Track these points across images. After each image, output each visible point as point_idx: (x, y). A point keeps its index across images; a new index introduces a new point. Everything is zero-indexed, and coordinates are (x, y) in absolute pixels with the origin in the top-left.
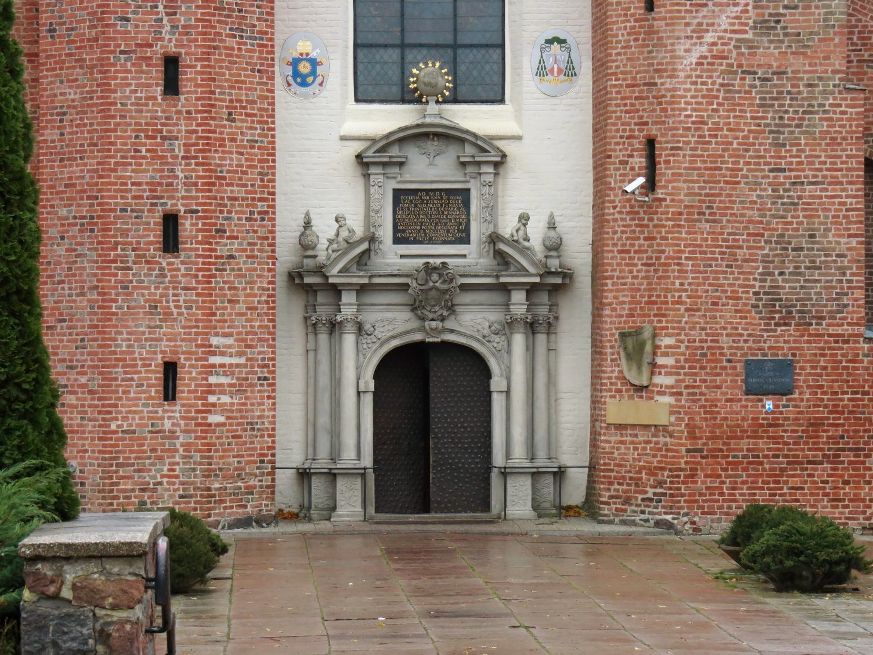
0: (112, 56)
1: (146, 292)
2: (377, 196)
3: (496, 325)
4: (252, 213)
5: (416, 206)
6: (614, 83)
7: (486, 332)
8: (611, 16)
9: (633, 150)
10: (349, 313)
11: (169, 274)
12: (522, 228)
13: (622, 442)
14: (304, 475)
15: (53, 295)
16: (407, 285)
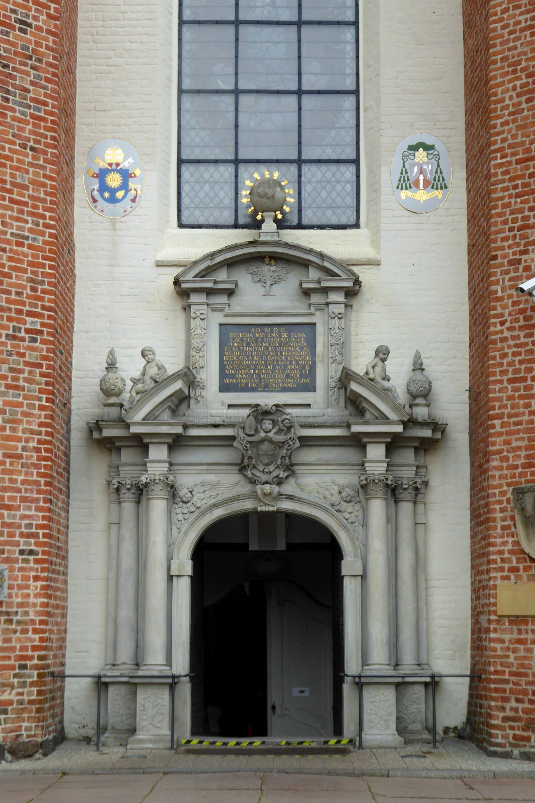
2: (199, 331)
3: (347, 490)
4: (16, 329)
6: (499, 161)
7: (336, 498)
8: (495, 77)
9: (526, 245)
10: (157, 473)
12: (380, 364)
13: (520, 641)
16: (233, 438)
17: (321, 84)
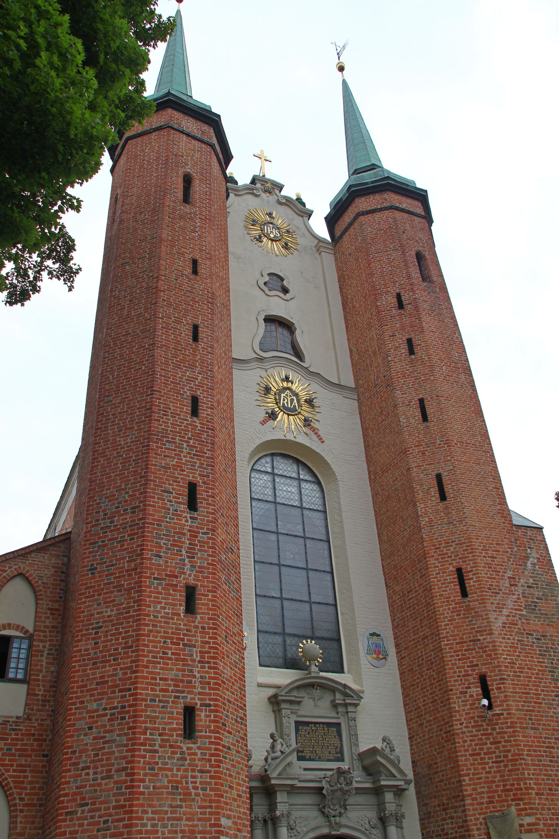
0: (148, 580)
1: (169, 773)
5: (309, 733)
11: (188, 758)
15: (76, 781)
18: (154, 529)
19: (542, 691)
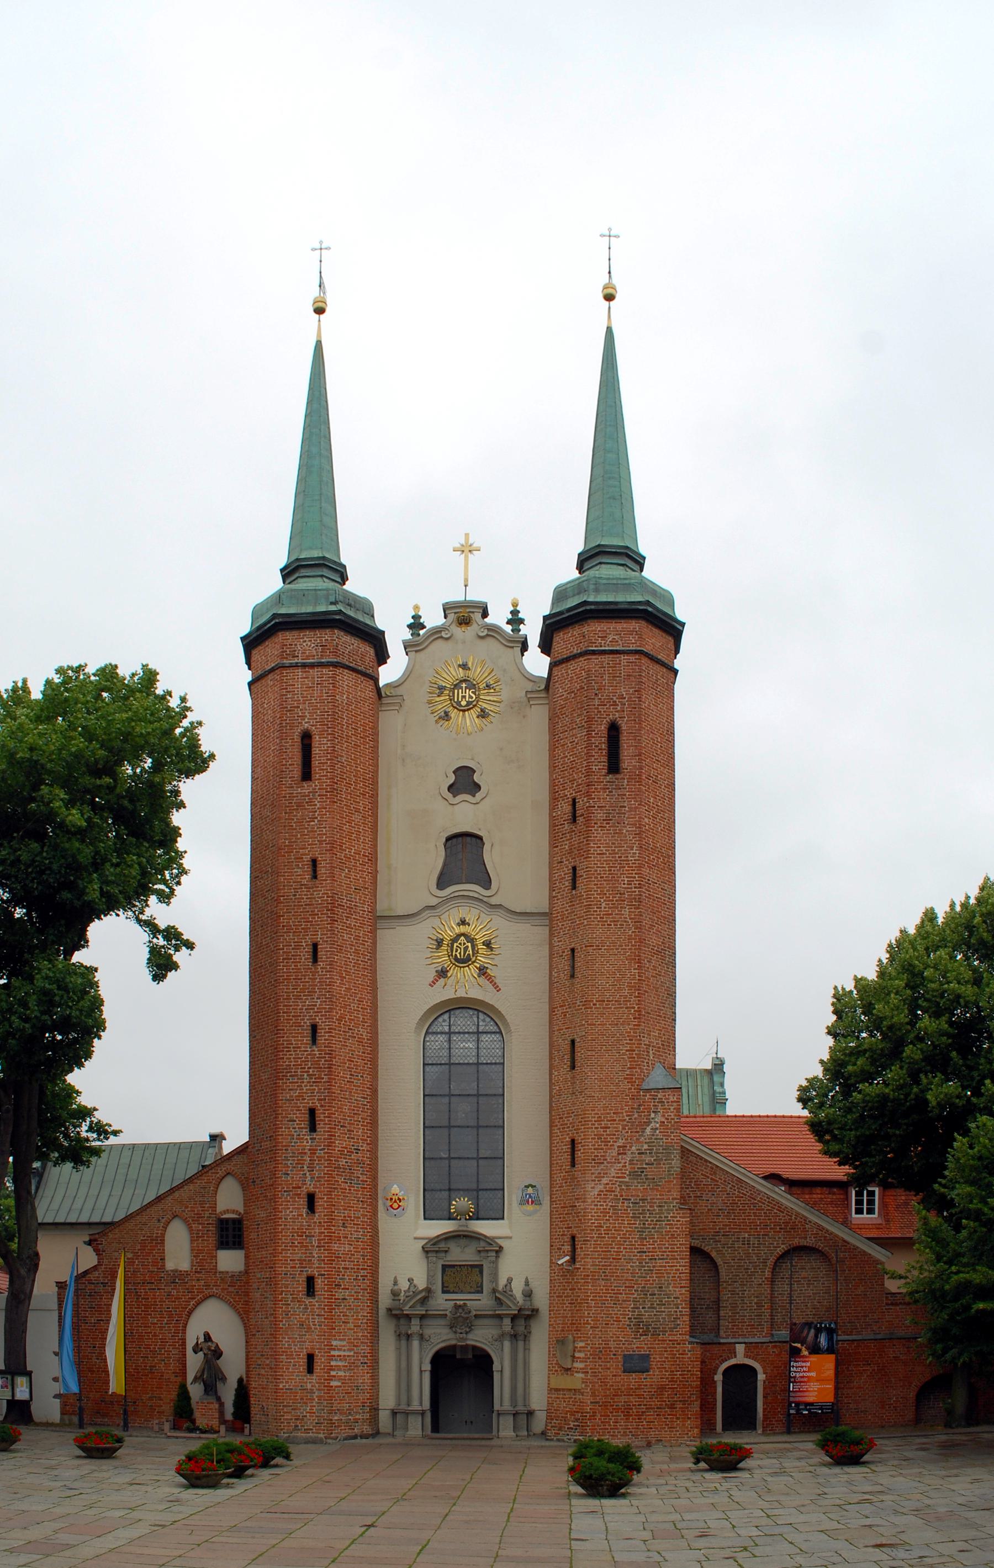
13: (558, 1398)
14: (394, 1413)
16: (446, 1315)
17: (488, 1154)
18: (283, 1153)
19: (624, 1248)
